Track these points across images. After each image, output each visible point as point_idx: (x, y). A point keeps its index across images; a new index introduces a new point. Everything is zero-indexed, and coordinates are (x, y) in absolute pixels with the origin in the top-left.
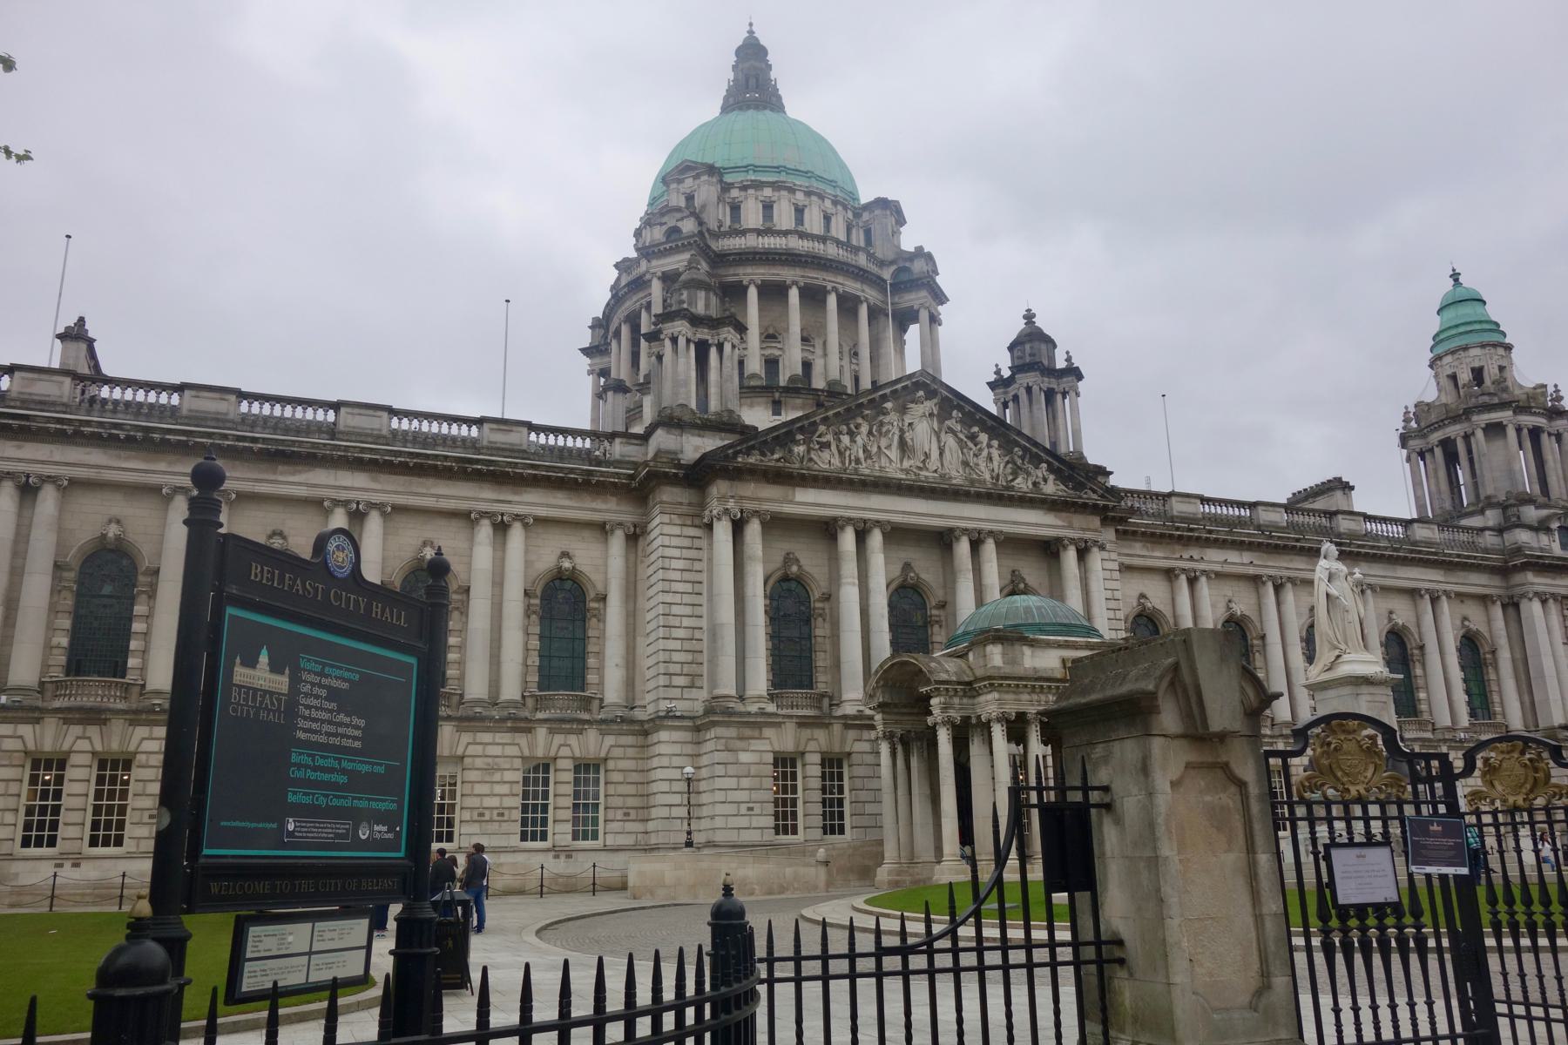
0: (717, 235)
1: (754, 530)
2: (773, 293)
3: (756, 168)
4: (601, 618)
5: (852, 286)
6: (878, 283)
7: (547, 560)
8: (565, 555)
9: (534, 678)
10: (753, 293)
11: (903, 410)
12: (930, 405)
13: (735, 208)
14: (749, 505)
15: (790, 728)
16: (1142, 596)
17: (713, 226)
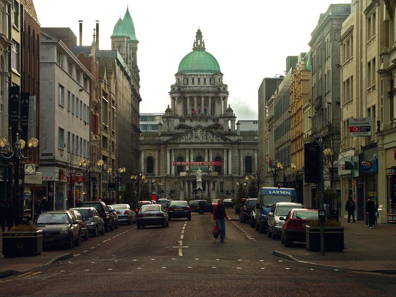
0: (182, 87)
1: (173, 151)
2: (192, 98)
3: (191, 71)
4: (155, 162)
5: (207, 95)
6: (212, 92)
7: (147, 155)
8: (150, 154)
9: (146, 171)
10: (188, 98)
11: (196, 131)
12: (200, 130)
13: (188, 80)
14: (172, 148)
15: (177, 179)
16: (248, 154)
17: (182, 85)
